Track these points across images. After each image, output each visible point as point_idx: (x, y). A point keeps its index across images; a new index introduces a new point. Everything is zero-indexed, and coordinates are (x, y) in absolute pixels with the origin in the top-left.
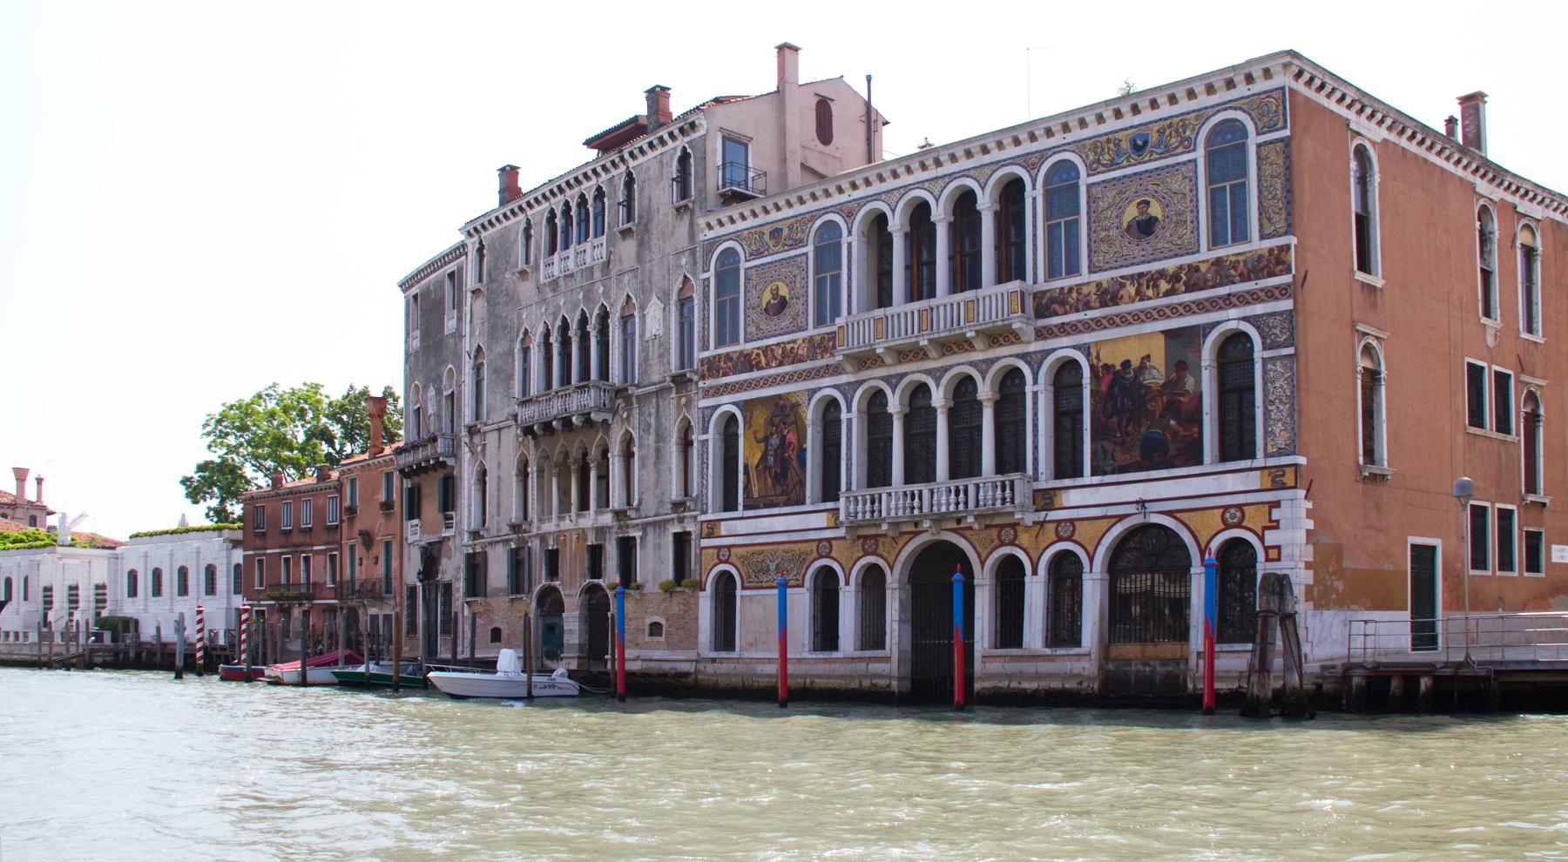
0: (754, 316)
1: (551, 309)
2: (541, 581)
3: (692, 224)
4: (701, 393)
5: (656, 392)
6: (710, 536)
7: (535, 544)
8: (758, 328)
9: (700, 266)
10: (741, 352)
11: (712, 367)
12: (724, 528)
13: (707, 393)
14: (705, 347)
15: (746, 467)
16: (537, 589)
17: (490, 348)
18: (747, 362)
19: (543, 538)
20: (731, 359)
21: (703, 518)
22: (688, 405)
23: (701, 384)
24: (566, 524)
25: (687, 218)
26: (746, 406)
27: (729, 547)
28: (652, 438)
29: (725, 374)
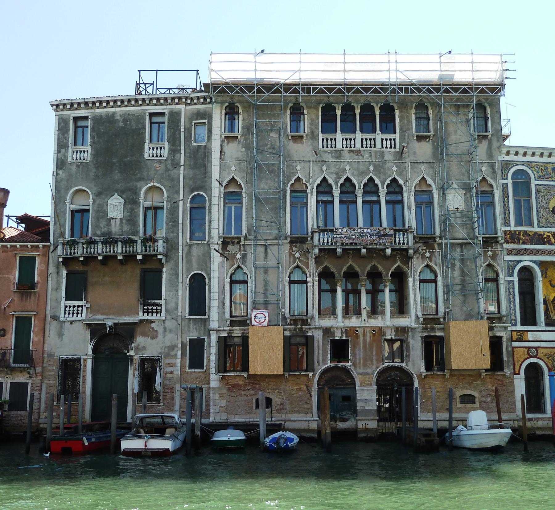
0: (544, 213)
1: (333, 170)
2: (324, 360)
3: (490, 148)
4: (505, 252)
5: (461, 245)
6: (520, 340)
7: (318, 336)
8: (547, 220)
9: (499, 173)
10: (536, 233)
11: (513, 237)
12: (530, 336)
13: (510, 252)
14: (507, 222)
15: (545, 301)
16: (320, 369)
17: (250, 183)
18: (540, 239)
19: (327, 331)
20: (528, 235)
21: (514, 328)
22: (494, 257)
23: (505, 246)
24: (354, 322)
25: (485, 143)
26: (541, 264)
27: (536, 348)
28: (457, 273)
29: (524, 243)
